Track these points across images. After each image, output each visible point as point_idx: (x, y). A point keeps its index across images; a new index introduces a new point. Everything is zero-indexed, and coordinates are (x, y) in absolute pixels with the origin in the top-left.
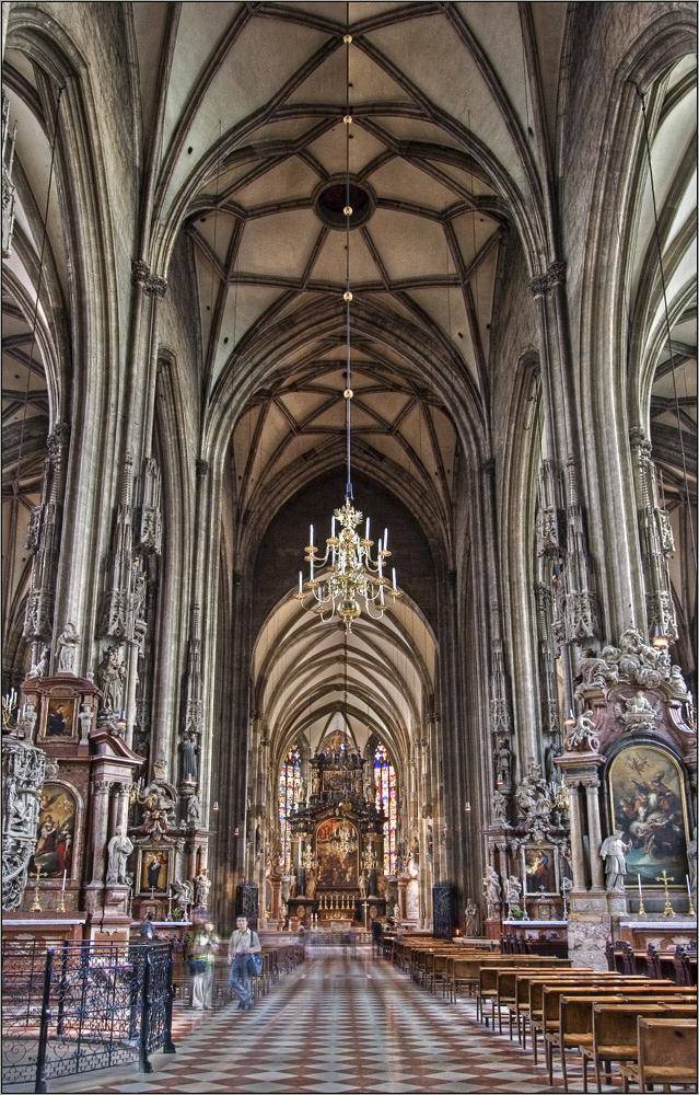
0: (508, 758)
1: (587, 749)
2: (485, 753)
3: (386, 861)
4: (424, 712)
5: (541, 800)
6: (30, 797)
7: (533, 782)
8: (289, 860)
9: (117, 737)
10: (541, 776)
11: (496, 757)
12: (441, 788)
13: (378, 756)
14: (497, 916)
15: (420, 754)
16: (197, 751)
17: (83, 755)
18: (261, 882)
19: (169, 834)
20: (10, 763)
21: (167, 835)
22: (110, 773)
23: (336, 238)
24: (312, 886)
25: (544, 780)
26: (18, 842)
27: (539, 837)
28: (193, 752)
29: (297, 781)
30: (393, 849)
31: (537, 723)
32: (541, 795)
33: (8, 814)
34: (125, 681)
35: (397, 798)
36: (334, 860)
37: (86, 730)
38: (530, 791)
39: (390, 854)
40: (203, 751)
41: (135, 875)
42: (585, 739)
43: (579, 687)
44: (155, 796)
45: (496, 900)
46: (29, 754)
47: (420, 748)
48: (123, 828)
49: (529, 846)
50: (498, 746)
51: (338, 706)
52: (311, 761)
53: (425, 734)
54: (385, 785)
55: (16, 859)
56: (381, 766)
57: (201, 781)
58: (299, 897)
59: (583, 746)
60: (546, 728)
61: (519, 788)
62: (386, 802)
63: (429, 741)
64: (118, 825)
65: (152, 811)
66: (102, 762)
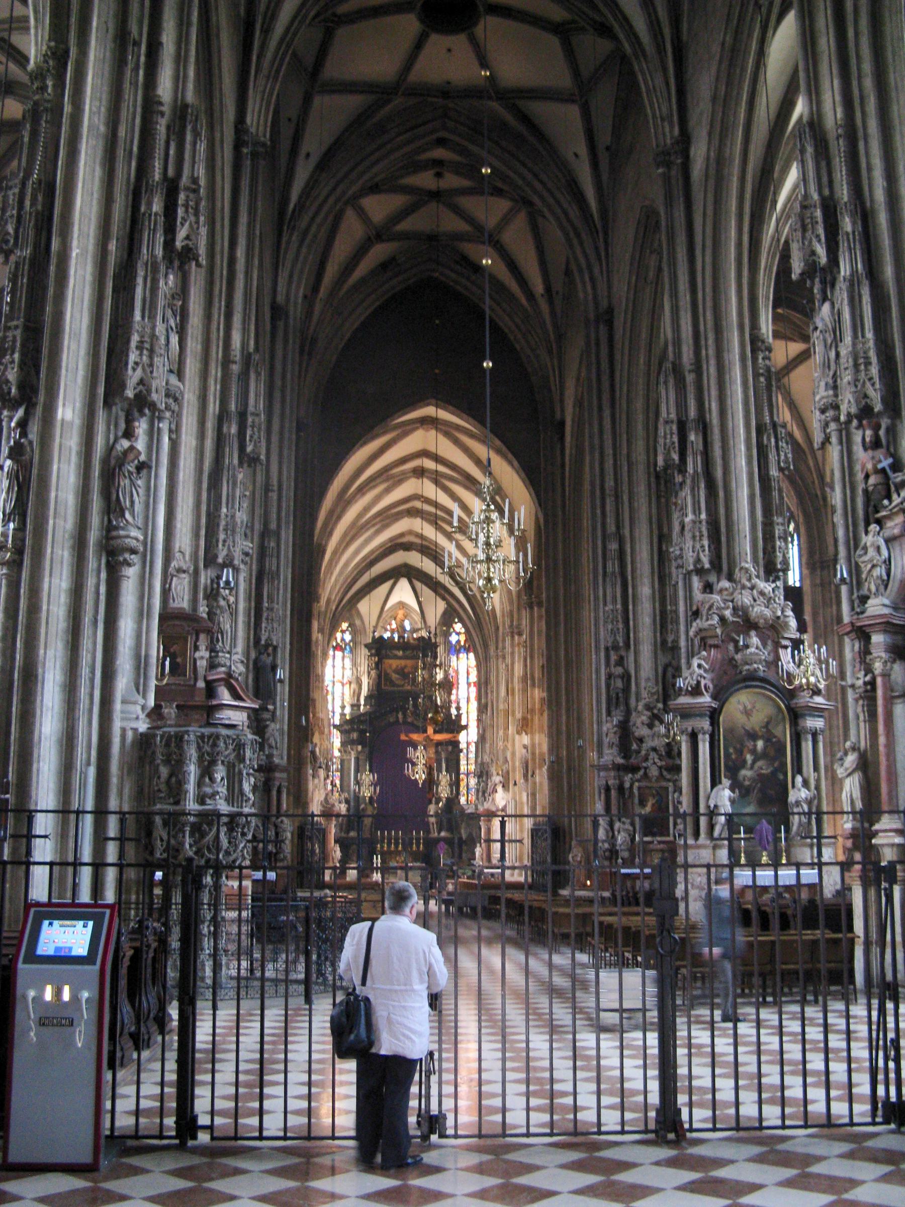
0: (622, 677)
1: (701, 694)
2: (598, 672)
3: (463, 784)
5: (656, 729)
7: (648, 707)
8: (338, 782)
10: (658, 701)
11: (609, 676)
12: (542, 700)
13: (454, 638)
15: (513, 646)
17: (200, 699)
23: (437, 42)
25: (660, 705)
27: (654, 772)
28: (269, 669)
30: (472, 768)
31: (655, 637)
32: (657, 723)
34: (234, 614)
35: (479, 698)
37: (201, 671)
39: (467, 775)
42: (698, 683)
43: (694, 624)
45: (606, 846)
47: (513, 637)
49: (643, 784)
50: (612, 662)
51: (403, 570)
52: (366, 646)
53: (519, 619)
55: (246, 830)
56: (458, 652)
57: (278, 704)
58: (353, 834)
59: (696, 691)
60: (664, 642)
61: (634, 714)
62: (463, 704)
66: (222, 706)
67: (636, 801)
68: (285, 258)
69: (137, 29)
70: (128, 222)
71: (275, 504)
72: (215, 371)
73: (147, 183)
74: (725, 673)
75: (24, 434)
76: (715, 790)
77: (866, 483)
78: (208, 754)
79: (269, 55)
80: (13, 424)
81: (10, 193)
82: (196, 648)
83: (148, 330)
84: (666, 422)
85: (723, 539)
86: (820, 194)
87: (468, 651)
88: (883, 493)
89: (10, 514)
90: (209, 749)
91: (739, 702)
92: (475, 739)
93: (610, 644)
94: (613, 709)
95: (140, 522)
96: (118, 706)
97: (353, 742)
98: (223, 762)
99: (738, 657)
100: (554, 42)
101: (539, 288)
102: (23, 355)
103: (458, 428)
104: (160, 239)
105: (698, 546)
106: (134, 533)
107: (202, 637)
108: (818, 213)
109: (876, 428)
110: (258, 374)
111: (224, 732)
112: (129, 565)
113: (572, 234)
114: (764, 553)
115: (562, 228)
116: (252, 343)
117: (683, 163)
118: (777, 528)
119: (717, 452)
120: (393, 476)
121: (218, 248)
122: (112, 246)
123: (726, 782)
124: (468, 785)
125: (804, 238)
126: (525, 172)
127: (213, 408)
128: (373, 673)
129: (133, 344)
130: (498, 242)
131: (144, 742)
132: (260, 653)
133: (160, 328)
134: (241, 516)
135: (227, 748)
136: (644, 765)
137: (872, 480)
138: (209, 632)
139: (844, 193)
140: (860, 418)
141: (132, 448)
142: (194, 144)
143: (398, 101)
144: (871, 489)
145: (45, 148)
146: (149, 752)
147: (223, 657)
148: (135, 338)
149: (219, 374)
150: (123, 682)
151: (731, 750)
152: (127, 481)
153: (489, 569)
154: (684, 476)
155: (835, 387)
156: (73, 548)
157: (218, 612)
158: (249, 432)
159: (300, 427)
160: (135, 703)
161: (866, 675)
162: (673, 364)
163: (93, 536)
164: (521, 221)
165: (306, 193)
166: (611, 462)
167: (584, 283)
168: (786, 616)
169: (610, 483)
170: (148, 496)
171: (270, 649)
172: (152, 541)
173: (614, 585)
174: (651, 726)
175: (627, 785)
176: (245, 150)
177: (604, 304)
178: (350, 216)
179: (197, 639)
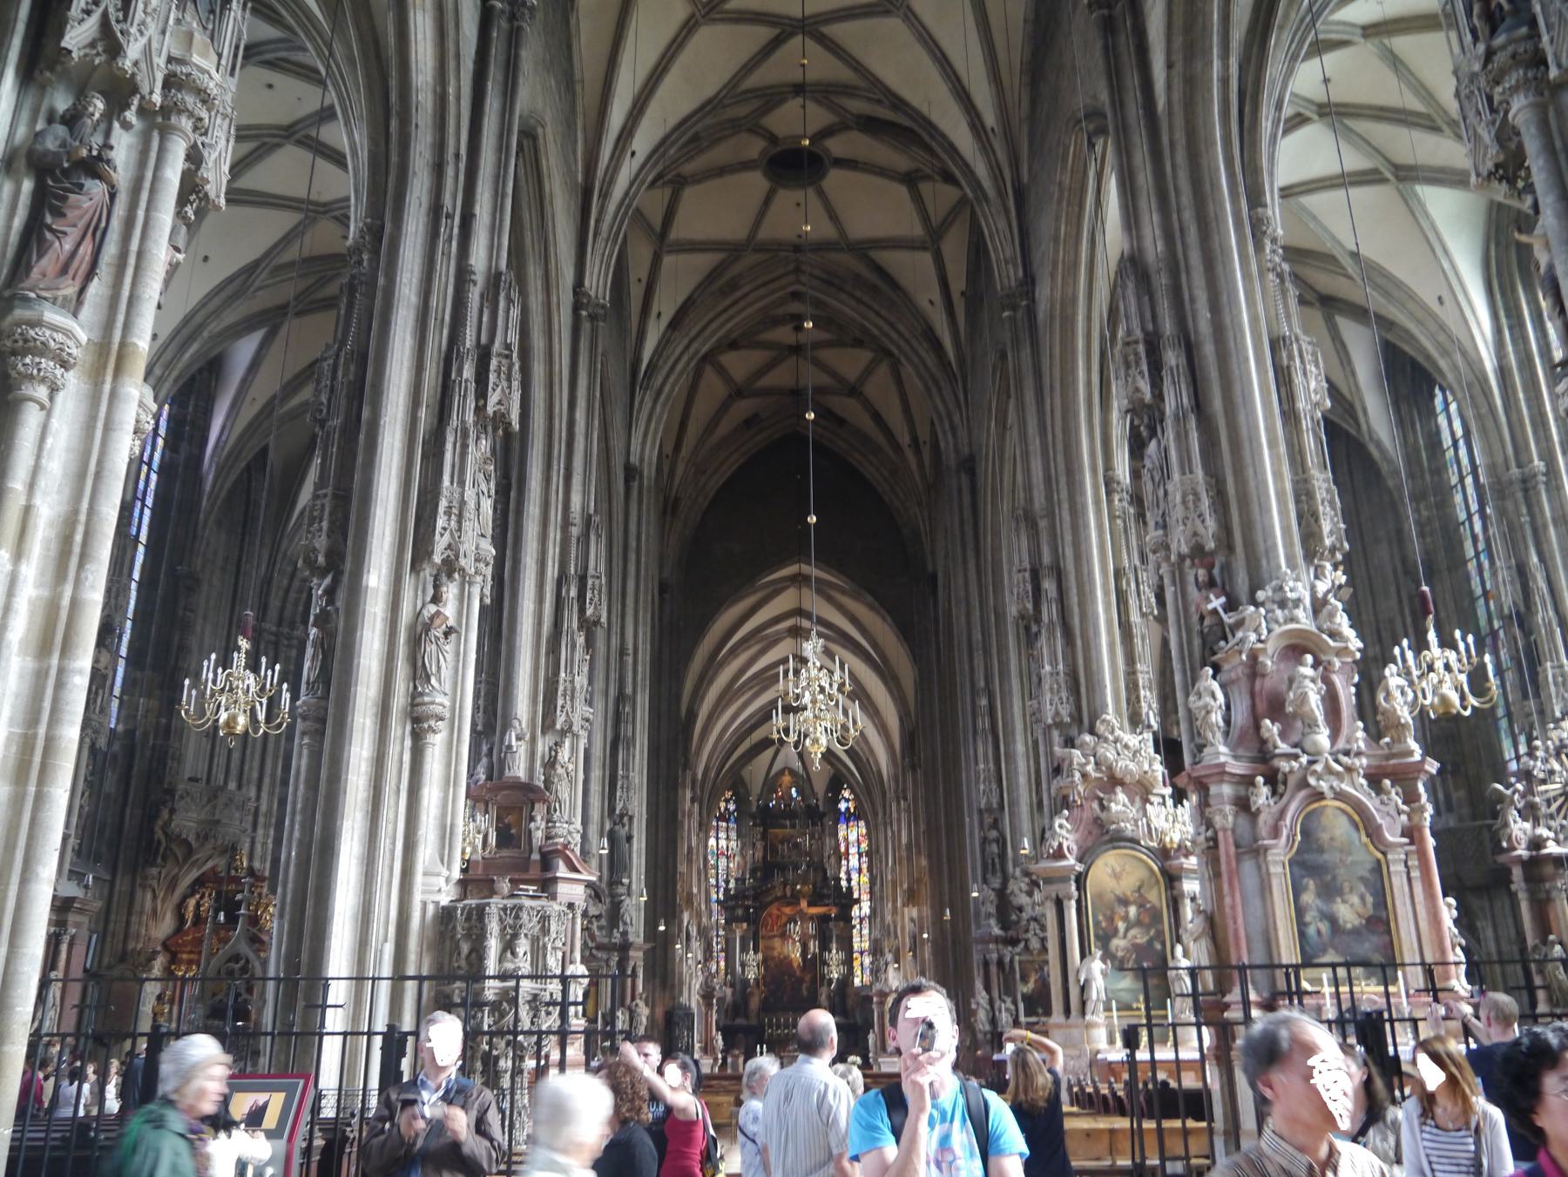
0: (998, 842)
2: (972, 834)
3: (856, 964)
4: (903, 758)
8: (722, 964)
11: (985, 841)
13: (843, 806)
14: (988, 1048)
16: (629, 838)
17: (534, 872)
19: (599, 947)
24: (755, 1003)
26: (551, 994)
29: (733, 844)
30: (866, 945)
31: (1031, 797)
35: (870, 869)
36: (786, 962)
38: (1023, 885)
39: (862, 953)
40: (635, 839)
42: (1060, 845)
45: (987, 1028)
47: (898, 803)
49: (1024, 958)
52: (753, 817)
54: (853, 850)
56: (848, 821)
58: (740, 1021)
61: (1012, 881)
62: (855, 876)
63: (910, 796)
66: (555, 880)
67: (1018, 976)
68: (637, 419)
69: (452, 201)
70: (439, 390)
71: (630, 668)
72: (555, 535)
73: (458, 350)
74: (1090, 833)
75: (331, 601)
76: (1085, 961)
77: (1202, 624)
79: (608, 218)
80: (320, 592)
81: (325, 364)
82: (532, 819)
83: (457, 496)
84: (1020, 571)
85: (1083, 690)
86: (1143, 329)
87: (858, 818)
88: (1220, 634)
89: (314, 682)
90: (511, 922)
91: (1106, 865)
92: (868, 911)
93: (983, 806)
94: (989, 876)
95: (448, 688)
96: (419, 879)
98: (526, 935)
99: (1103, 816)
100: (902, 191)
101: (904, 439)
102: (332, 523)
103: (830, 585)
104: (471, 403)
105: (1056, 699)
106: (440, 699)
107: (537, 806)
108: (1141, 348)
109: (1210, 567)
110: (598, 536)
111: (528, 903)
112: (434, 731)
113: (930, 383)
114: (1128, 703)
115: (921, 378)
116: (592, 504)
117: (1028, 306)
118: (1140, 676)
119: (1074, 599)
120: (767, 637)
121: (557, 410)
122: (423, 413)
123: (1099, 953)
124: (862, 964)
125: (1127, 375)
126: (881, 323)
127: (552, 571)
128: (759, 845)
129: (441, 509)
130: (861, 393)
131: (445, 916)
132: (615, 824)
133: (470, 494)
134: (581, 681)
135: (530, 920)
136: (1026, 936)
137: (1207, 622)
139: (1168, 327)
140: (1192, 558)
141: (438, 613)
142: (507, 311)
143: (750, 259)
144: (1206, 630)
145: (359, 319)
146: (450, 927)
147: (561, 828)
148: (443, 504)
149: (558, 537)
150: (426, 852)
151: (1101, 918)
152: (434, 647)
153: (815, 728)
154: (1039, 626)
155: (1165, 527)
156: (376, 715)
158: (589, 595)
159: (663, 587)
160: (438, 875)
161: (1207, 830)
162: (1025, 510)
163: (399, 700)
164: (883, 369)
165: (659, 351)
166: (978, 614)
167: (944, 432)
168: (1153, 771)
169: (977, 636)
170: (458, 661)
171: (626, 819)
172: (460, 707)
173: (985, 743)
174: (1030, 894)
175: (1007, 959)
176: (584, 313)
177: (966, 450)
178: (709, 374)
179: (533, 809)
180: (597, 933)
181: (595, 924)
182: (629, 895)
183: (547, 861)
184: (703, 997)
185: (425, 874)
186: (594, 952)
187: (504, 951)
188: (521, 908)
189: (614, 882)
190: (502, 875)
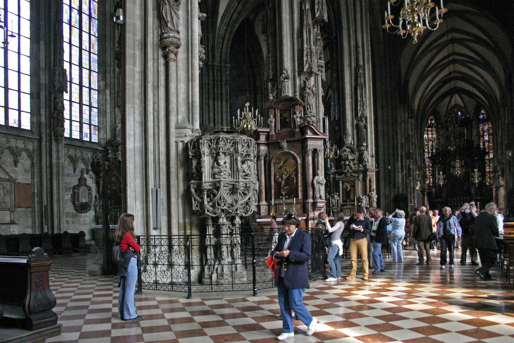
6: (249, 162)
8: (431, 180)
9: (312, 125)
18: (414, 193)
20: (236, 147)
21: (353, 173)
22: (311, 145)
24: (444, 194)
26: (246, 184)
33: (238, 171)
41: (339, 194)
44: (345, 153)
46: (246, 141)
48: (321, 172)
55: (246, 192)
58: (439, 200)
64: (318, 170)
65: (344, 161)
66: (306, 139)
78: (215, 149)
82: (295, 113)
90: (215, 146)
97: (437, 163)
98: (224, 153)
107: (296, 107)
111: (222, 136)
138: (300, 105)
157: (306, 96)
179: (295, 109)
180: (353, 166)
181: (352, 163)
182: (367, 150)
183: (303, 130)
184: (421, 192)
185: (178, 128)
186: (352, 174)
187: (214, 163)
188: (219, 139)
189: (359, 145)
190: (283, 139)
